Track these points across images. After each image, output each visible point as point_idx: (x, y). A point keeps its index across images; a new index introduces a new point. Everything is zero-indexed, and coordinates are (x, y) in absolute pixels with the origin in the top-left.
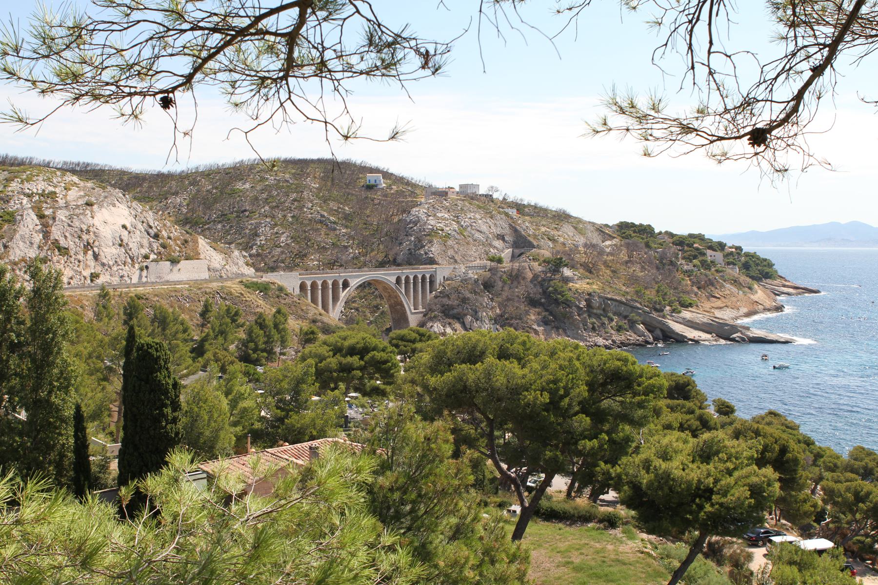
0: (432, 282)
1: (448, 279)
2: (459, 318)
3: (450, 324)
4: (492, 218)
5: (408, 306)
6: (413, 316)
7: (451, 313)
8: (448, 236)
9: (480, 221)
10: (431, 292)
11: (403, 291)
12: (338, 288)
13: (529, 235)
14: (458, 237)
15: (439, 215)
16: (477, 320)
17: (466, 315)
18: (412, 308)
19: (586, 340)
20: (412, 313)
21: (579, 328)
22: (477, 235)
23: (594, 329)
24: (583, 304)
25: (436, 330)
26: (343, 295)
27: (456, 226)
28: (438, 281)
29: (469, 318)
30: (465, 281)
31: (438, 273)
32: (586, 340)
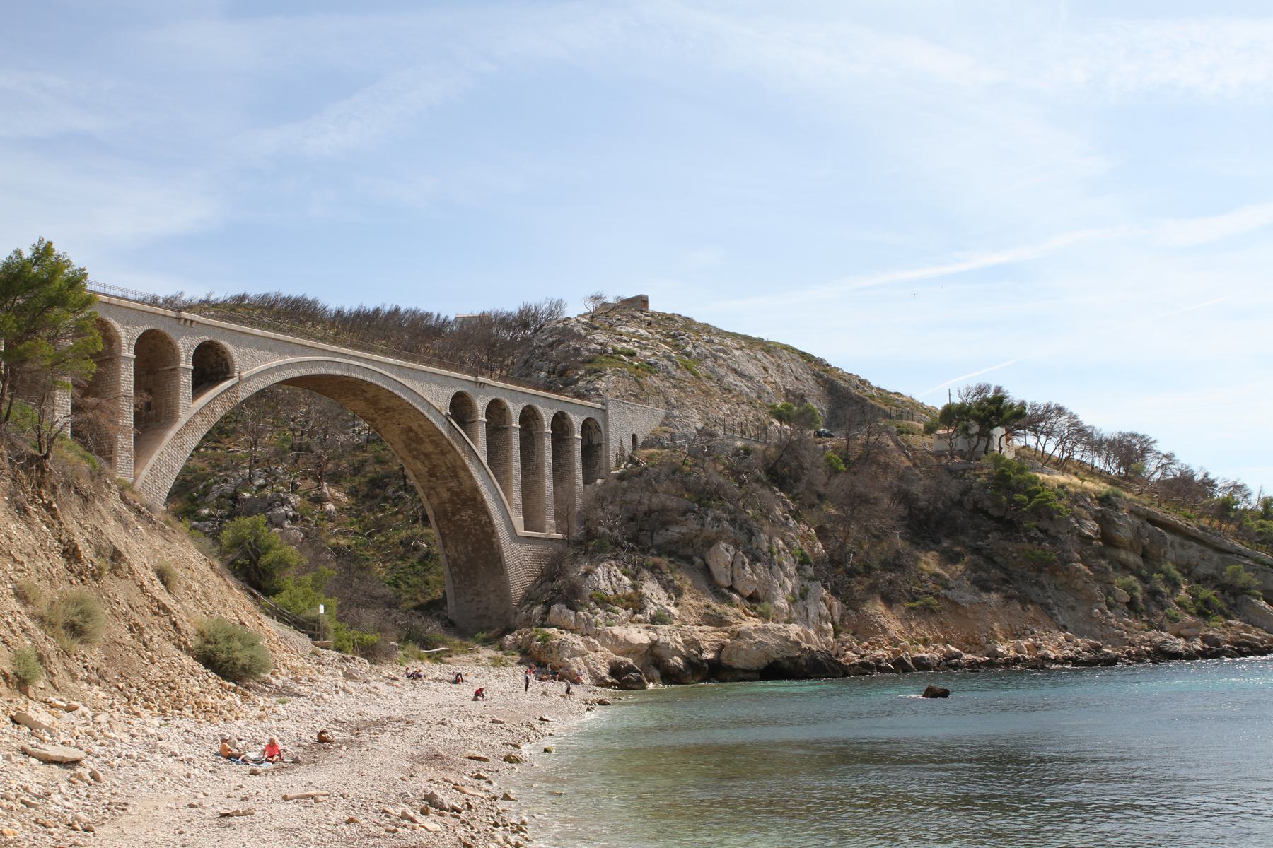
0: (591, 450)
1: (645, 445)
3: (654, 569)
4: (768, 351)
5: (504, 511)
6: (520, 549)
7: (659, 538)
8: (650, 367)
9: (738, 353)
10: (588, 479)
11: (481, 451)
12: (174, 372)
13: (872, 397)
14: (678, 374)
16: (755, 559)
17: (710, 543)
18: (518, 520)
19: (1124, 642)
20: (517, 538)
21: (1091, 600)
22: (731, 378)
23: (1132, 606)
24: (1091, 528)
25: (603, 585)
26: (193, 411)
28: (614, 447)
29: (722, 555)
31: (613, 419)
32: (1124, 642)
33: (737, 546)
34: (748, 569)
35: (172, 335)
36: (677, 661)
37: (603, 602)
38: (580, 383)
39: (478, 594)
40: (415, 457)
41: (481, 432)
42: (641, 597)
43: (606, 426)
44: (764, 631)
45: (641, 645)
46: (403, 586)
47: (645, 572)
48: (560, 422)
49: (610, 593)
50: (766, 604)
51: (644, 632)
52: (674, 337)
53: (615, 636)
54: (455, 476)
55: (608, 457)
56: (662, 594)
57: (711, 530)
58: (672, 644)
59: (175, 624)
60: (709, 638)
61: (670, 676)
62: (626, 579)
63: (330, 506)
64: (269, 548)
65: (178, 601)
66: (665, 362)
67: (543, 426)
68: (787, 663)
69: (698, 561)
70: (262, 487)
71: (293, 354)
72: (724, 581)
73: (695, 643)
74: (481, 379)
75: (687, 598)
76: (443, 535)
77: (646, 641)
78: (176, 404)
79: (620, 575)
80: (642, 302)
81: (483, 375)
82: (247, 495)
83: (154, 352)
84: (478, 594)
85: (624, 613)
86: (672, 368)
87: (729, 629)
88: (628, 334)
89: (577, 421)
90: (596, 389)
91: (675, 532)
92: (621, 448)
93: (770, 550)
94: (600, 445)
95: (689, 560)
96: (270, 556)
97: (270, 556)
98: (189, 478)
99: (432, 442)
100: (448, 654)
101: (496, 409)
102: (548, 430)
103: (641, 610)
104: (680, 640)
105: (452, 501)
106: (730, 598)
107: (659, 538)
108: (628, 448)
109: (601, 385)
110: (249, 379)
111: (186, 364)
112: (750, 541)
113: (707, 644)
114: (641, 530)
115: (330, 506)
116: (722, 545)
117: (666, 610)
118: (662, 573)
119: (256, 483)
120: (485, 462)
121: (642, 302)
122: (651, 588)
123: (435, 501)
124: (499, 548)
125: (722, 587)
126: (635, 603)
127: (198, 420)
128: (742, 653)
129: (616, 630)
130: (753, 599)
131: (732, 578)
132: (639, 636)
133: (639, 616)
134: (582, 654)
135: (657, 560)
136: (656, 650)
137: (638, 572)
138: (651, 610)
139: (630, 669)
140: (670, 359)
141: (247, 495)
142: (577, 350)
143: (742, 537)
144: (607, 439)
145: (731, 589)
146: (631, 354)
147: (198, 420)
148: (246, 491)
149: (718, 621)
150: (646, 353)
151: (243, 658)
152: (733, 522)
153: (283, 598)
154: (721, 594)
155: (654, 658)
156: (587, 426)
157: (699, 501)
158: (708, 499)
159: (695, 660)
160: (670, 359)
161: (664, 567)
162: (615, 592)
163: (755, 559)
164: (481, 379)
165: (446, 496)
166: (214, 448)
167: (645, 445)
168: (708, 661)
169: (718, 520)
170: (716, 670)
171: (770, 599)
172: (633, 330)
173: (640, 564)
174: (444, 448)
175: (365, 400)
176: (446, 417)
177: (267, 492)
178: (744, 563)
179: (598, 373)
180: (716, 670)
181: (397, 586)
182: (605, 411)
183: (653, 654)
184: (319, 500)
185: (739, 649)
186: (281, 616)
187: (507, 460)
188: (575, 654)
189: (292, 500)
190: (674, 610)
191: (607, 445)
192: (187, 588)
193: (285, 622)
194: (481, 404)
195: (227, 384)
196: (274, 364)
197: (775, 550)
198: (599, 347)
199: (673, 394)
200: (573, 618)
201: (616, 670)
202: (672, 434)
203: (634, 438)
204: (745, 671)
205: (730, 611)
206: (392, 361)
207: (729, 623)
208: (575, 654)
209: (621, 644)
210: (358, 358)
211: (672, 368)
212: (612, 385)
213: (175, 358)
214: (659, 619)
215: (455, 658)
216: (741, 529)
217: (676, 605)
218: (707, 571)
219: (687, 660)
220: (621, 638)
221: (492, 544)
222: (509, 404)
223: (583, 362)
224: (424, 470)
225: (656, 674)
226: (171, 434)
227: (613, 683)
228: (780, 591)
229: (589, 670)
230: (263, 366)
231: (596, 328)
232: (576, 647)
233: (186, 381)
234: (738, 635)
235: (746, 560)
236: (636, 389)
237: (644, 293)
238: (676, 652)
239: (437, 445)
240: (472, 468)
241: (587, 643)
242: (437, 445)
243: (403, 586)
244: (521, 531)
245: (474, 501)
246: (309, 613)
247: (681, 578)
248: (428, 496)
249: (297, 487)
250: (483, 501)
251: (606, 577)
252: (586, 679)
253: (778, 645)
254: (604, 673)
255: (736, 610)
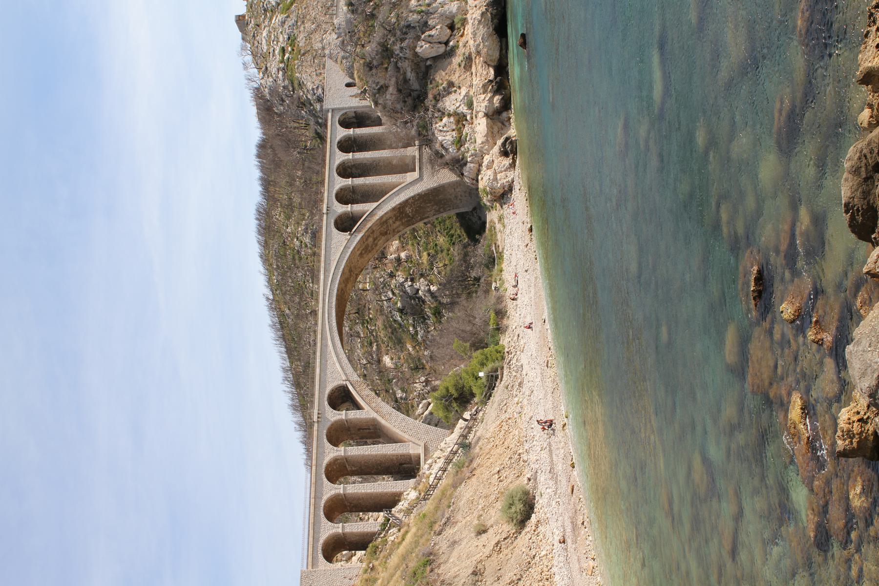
2: (426, 69)
3: (437, 98)
7: (415, 85)
8: (292, 40)
10: (378, 122)
11: (369, 207)
14: (293, 17)
15: (265, 48)
17: (416, 54)
27: (278, 18)
29: (424, 48)
30: (350, 36)
33: (418, 38)
34: (433, 32)
35: (328, 425)
36: (497, 99)
37: (460, 142)
38: (309, 97)
39: (456, 197)
40: (376, 245)
41: (357, 208)
42: (456, 114)
43: (343, 109)
44: (474, 34)
45: (487, 124)
46: (452, 232)
47: (439, 105)
48: (346, 146)
49: (454, 133)
50: (456, 20)
51: (478, 121)
52: (265, 10)
53: (482, 143)
54: (386, 222)
55: (363, 107)
56: (453, 96)
57: (408, 53)
58: (486, 103)
59: (505, 539)
60: (483, 73)
61: (506, 105)
62: (445, 120)
63: (403, 255)
64: (447, 389)
65: (492, 526)
66: (286, 26)
67: (348, 160)
68: (495, 21)
69: (429, 63)
70: (393, 294)
71: (327, 345)
72: (442, 49)
73: (484, 86)
74: (325, 211)
75: (454, 78)
76: (421, 220)
77: (484, 120)
78: (366, 419)
79: (441, 124)
80: (241, 21)
81: (321, 210)
82: (399, 305)
83: (338, 434)
84: (456, 197)
85: (466, 130)
86: (290, 22)
87: (473, 56)
88: (268, 45)
89: (342, 133)
90: (313, 89)
91: (410, 75)
92: (355, 96)
93: (419, 13)
94: (355, 112)
95: (428, 68)
96: (452, 391)
97: (452, 391)
98: (390, 330)
99: (367, 240)
100: (497, 247)
101: (344, 197)
102: (350, 156)
103: (465, 116)
104: (483, 96)
105: (401, 220)
106: (453, 47)
107: (415, 85)
108: (355, 90)
109: (310, 86)
110: (346, 374)
111: (341, 415)
112: (414, 28)
113: (485, 73)
114: (410, 95)
115: (403, 255)
116: (418, 50)
117: (464, 98)
118: (439, 94)
119: (391, 296)
120: (376, 204)
121: (241, 21)
122: (451, 103)
123: (402, 227)
124: (428, 190)
125: (446, 51)
126: (460, 119)
127: (374, 405)
128: (490, 52)
129: (480, 138)
130: (452, 27)
131: (440, 43)
132: (481, 126)
133: (468, 118)
134: (495, 174)
135: (430, 96)
136: (490, 113)
137: (439, 111)
138: (464, 109)
139: (504, 144)
140: (283, 23)
141: (399, 305)
142: (284, 87)
143: (411, 34)
144: (351, 108)
145: (446, 43)
146: (283, 50)
147: (374, 405)
148: (396, 303)
149: (469, 61)
150: (281, 39)
151: (519, 506)
152: (402, 40)
153: (475, 390)
154: (450, 53)
155: (498, 116)
156: (345, 123)
157: (389, 59)
158: (387, 49)
159: (495, 87)
160: (283, 23)
161: (435, 91)
162: (453, 130)
163: (425, 26)
164: (325, 211)
165: (398, 223)
166: (369, 309)
167: (352, 77)
168: (496, 77)
169: (402, 48)
170: (501, 69)
171: (452, 17)
172: (264, 41)
173: (434, 106)
174: (371, 231)
175: (346, 286)
176: (351, 235)
177: (397, 292)
178: (430, 36)
179: (301, 85)
180: (501, 69)
181: (452, 236)
182: (333, 110)
183: (493, 115)
184: (398, 260)
185: (488, 54)
186: (488, 396)
187: (373, 186)
188: (495, 179)
189: (402, 280)
190: (463, 91)
191: (354, 108)
192: (484, 510)
193: (490, 396)
194: (341, 209)
195: (350, 388)
196: (335, 359)
197: (419, 9)
198: (281, 73)
199: (308, 25)
200: (472, 165)
201: (505, 154)
202: (343, 58)
203: (348, 85)
204: (501, 50)
205: (461, 51)
206: (322, 277)
207: (470, 54)
208: (495, 179)
209: (487, 140)
210: (324, 300)
211: (290, 22)
212: (309, 78)
213: (341, 421)
214: (470, 105)
215: (499, 243)
216: (406, 33)
217: (460, 88)
218: (435, 59)
219: (496, 92)
220: (484, 139)
221: (426, 194)
222: (337, 187)
223: (293, 87)
224: (383, 238)
225: (504, 114)
226: (383, 422)
227: (513, 158)
228: (446, 7)
229: (505, 171)
230: (337, 365)
231: (266, 68)
232: (492, 178)
233: (353, 415)
234: (478, 53)
235: (427, 33)
236: (309, 57)
237: (233, 19)
238: (491, 100)
239: (369, 236)
240: (380, 213)
241: (488, 167)
242: (369, 236)
243: (452, 232)
244: (415, 175)
245: (400, 211)
246: (484, 380)
247: (441, 77)
248: (398, 232)
249: (392, 272)
250: (400, 204)
251: (444, 133)
252: (511, 175)
253: (484, 27)
254: (507, 161)
255: (461, 44)
